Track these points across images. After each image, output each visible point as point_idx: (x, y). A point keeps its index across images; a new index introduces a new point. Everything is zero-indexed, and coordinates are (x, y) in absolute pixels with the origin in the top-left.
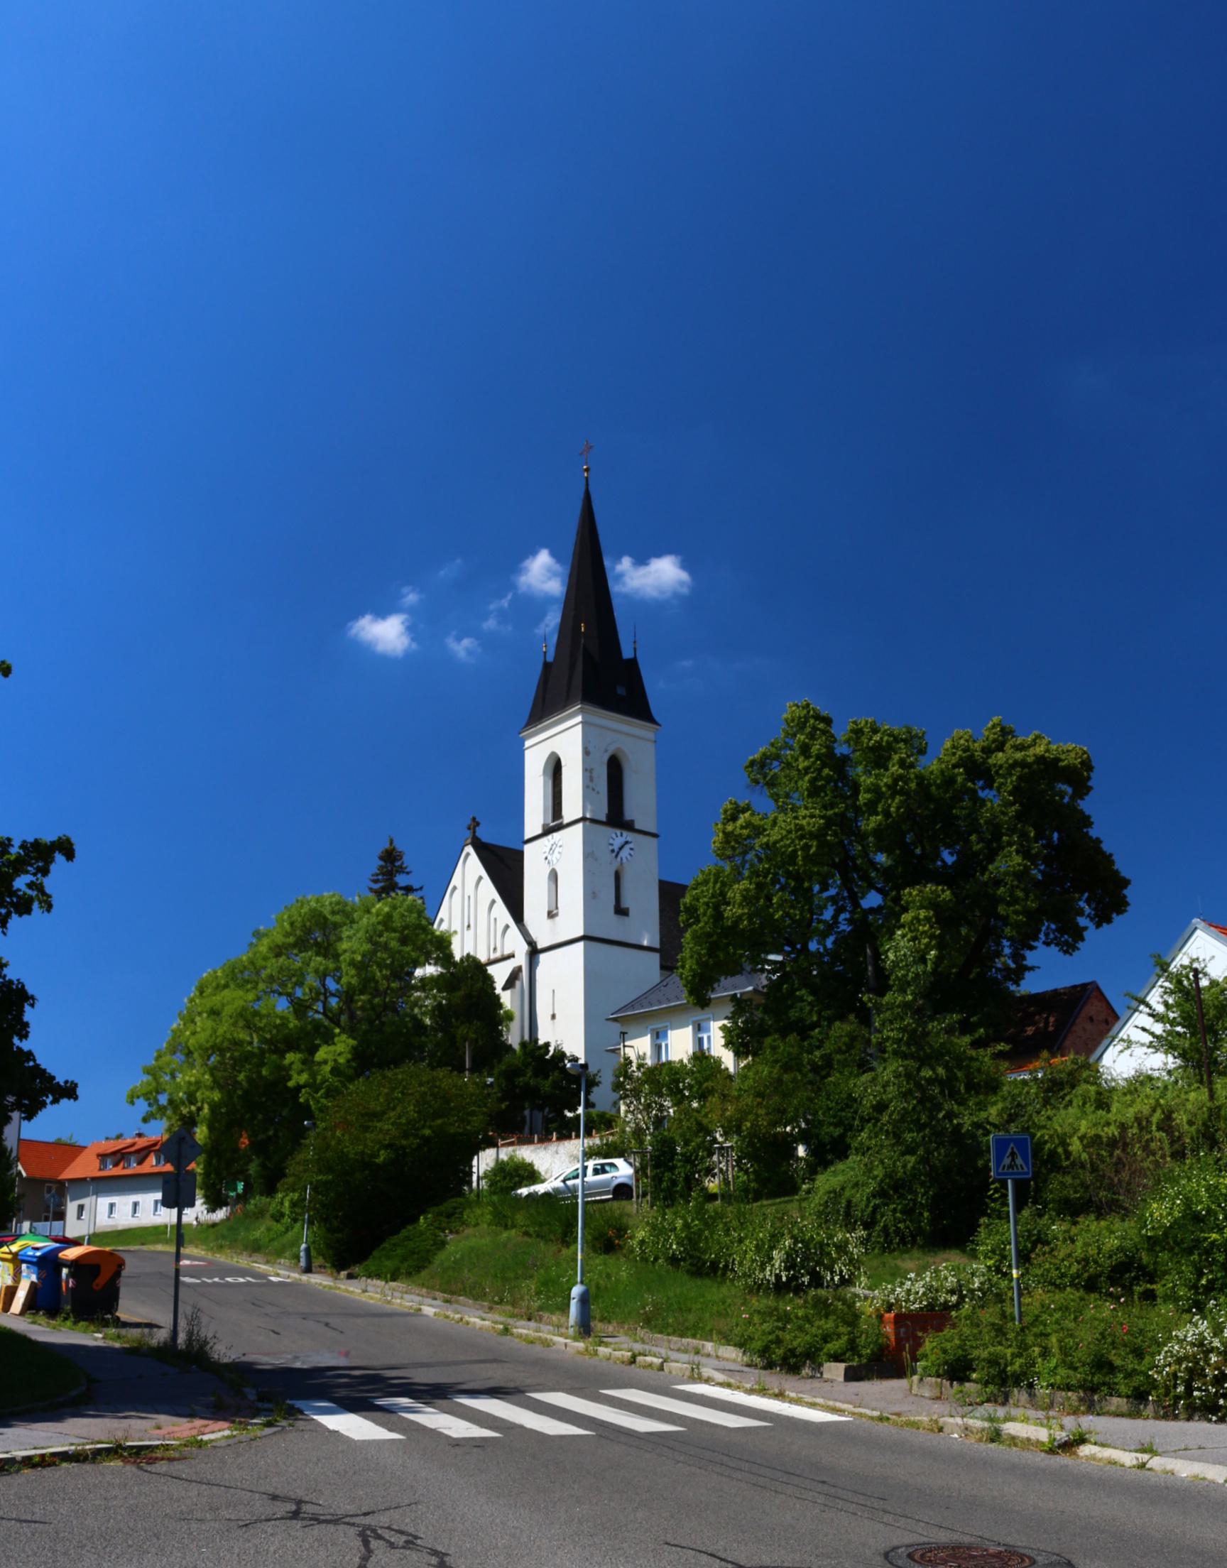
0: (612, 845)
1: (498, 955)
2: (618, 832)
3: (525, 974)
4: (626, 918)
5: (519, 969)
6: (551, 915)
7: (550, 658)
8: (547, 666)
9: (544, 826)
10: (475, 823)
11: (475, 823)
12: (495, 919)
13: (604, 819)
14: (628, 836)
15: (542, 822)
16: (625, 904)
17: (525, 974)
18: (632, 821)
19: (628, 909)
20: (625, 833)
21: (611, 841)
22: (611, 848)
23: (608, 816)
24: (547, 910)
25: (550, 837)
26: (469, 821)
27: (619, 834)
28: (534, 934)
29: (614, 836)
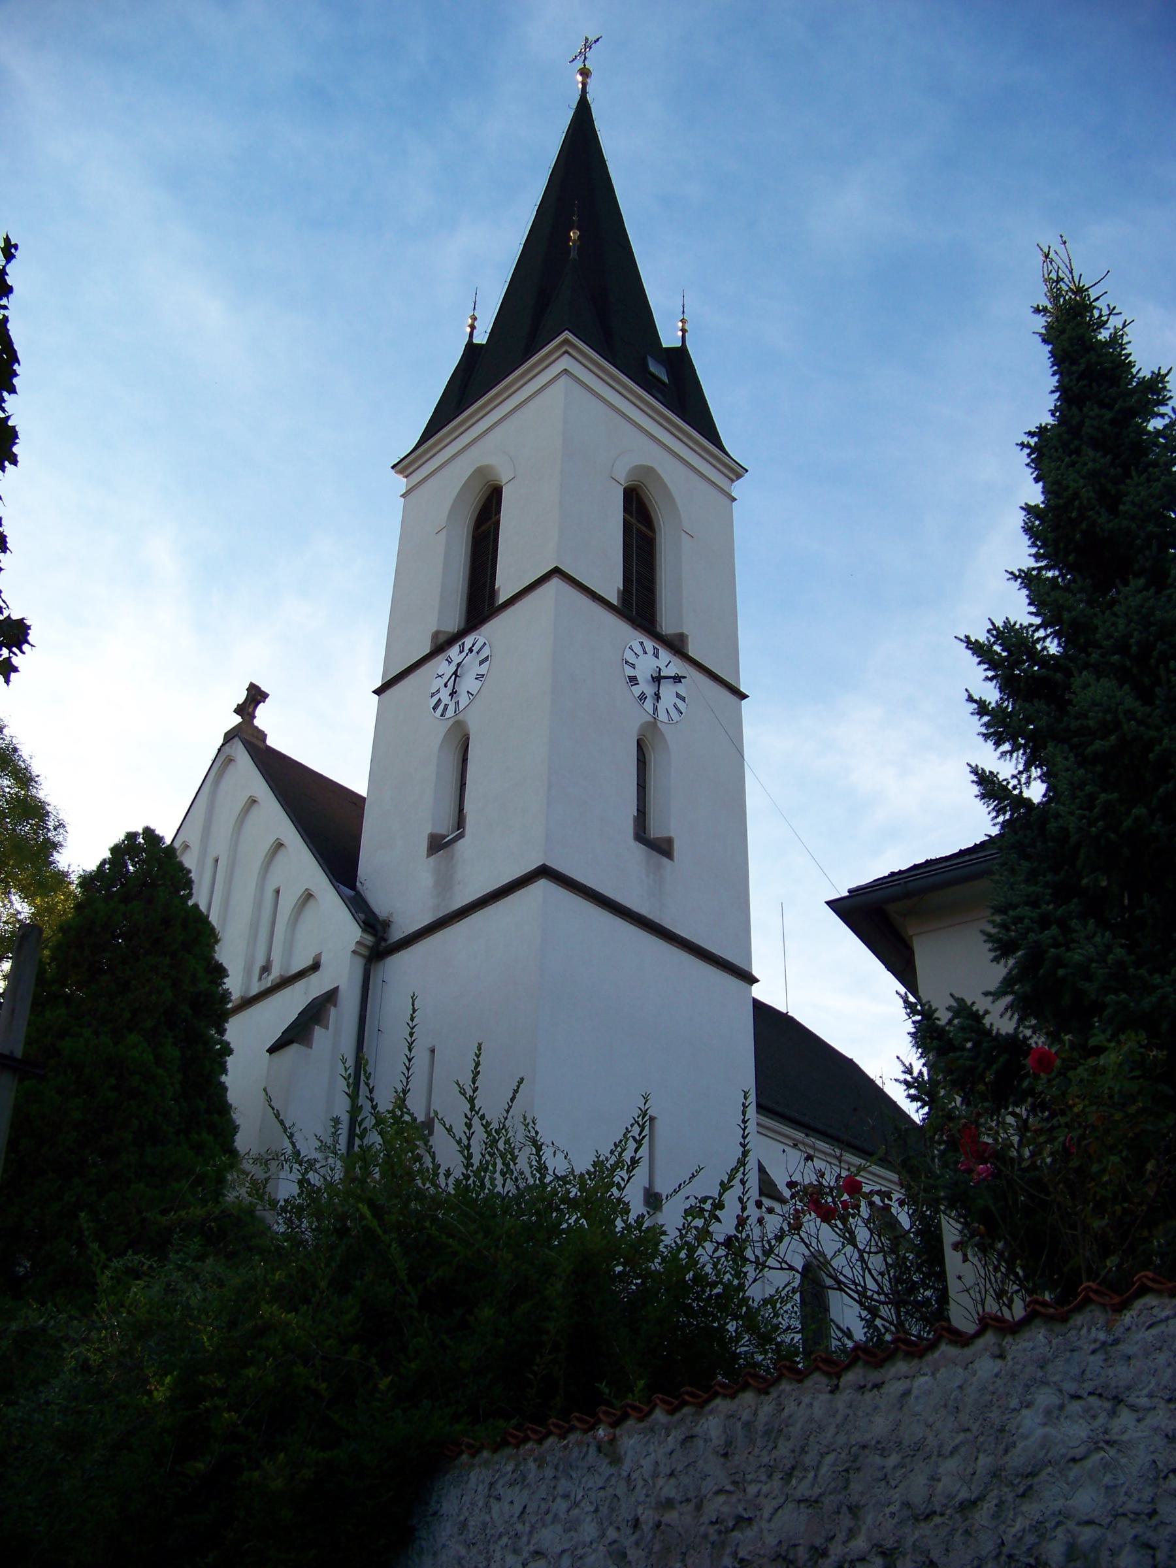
0: (633, 666)
1: (276, 973)
2: (649, 644)
3: (345, 1014)
4: (665, 860)
5: (331, 997)
6: (437, 844)
7: (481, 338)
8: (471, 348)
9: (436, 635)
10: (256, 696)
11: (256, 696)
12: (278, 892)
13: (615, 601)
14: (670, 665)
15: (435, 629)
16: (655, 831)
17: (345, 1014)
18: (682, 637)
19: (669, 841)
20: (665, 655)
21: (631, 658)
22: (630, 672)
23: (625, 593)
24: (428, 829)
25: (454, 652)
26: (241, 697)
27: (650, 650)
28: (381, 902)
29: (639, 650)
